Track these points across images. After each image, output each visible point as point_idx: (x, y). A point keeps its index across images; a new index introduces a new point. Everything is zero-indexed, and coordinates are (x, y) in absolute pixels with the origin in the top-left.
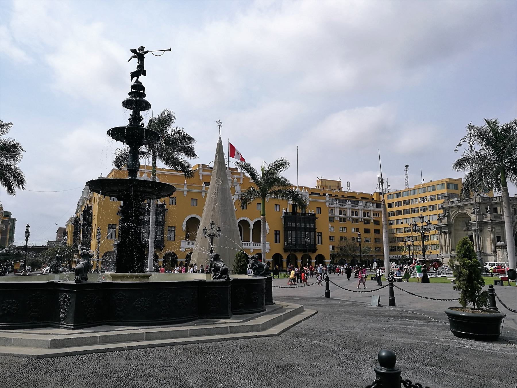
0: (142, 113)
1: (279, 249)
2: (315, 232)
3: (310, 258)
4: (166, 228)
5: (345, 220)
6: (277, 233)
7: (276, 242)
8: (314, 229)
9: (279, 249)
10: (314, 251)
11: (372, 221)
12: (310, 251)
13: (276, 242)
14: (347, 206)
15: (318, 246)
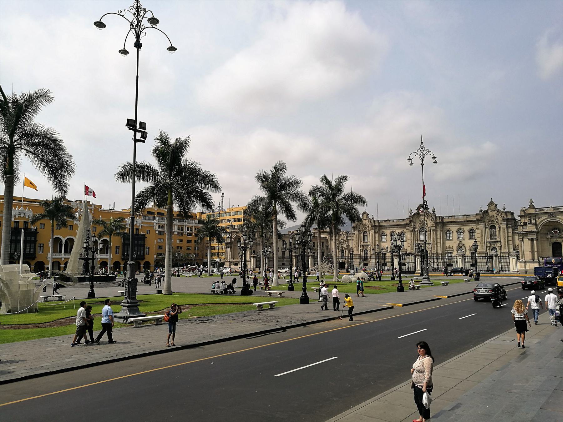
1: (118, 258)
2: (144, 246)
3: (140, 264)
4: (37, 245)
5: (182, 234)
6: (117, 247)
7: (116, 253)
8: (144, 245)
9: (118, 258)
10: (143, 259)
12: (140, 259)
13: (116, 253)
14: (184, 224)
15: (147, 256)
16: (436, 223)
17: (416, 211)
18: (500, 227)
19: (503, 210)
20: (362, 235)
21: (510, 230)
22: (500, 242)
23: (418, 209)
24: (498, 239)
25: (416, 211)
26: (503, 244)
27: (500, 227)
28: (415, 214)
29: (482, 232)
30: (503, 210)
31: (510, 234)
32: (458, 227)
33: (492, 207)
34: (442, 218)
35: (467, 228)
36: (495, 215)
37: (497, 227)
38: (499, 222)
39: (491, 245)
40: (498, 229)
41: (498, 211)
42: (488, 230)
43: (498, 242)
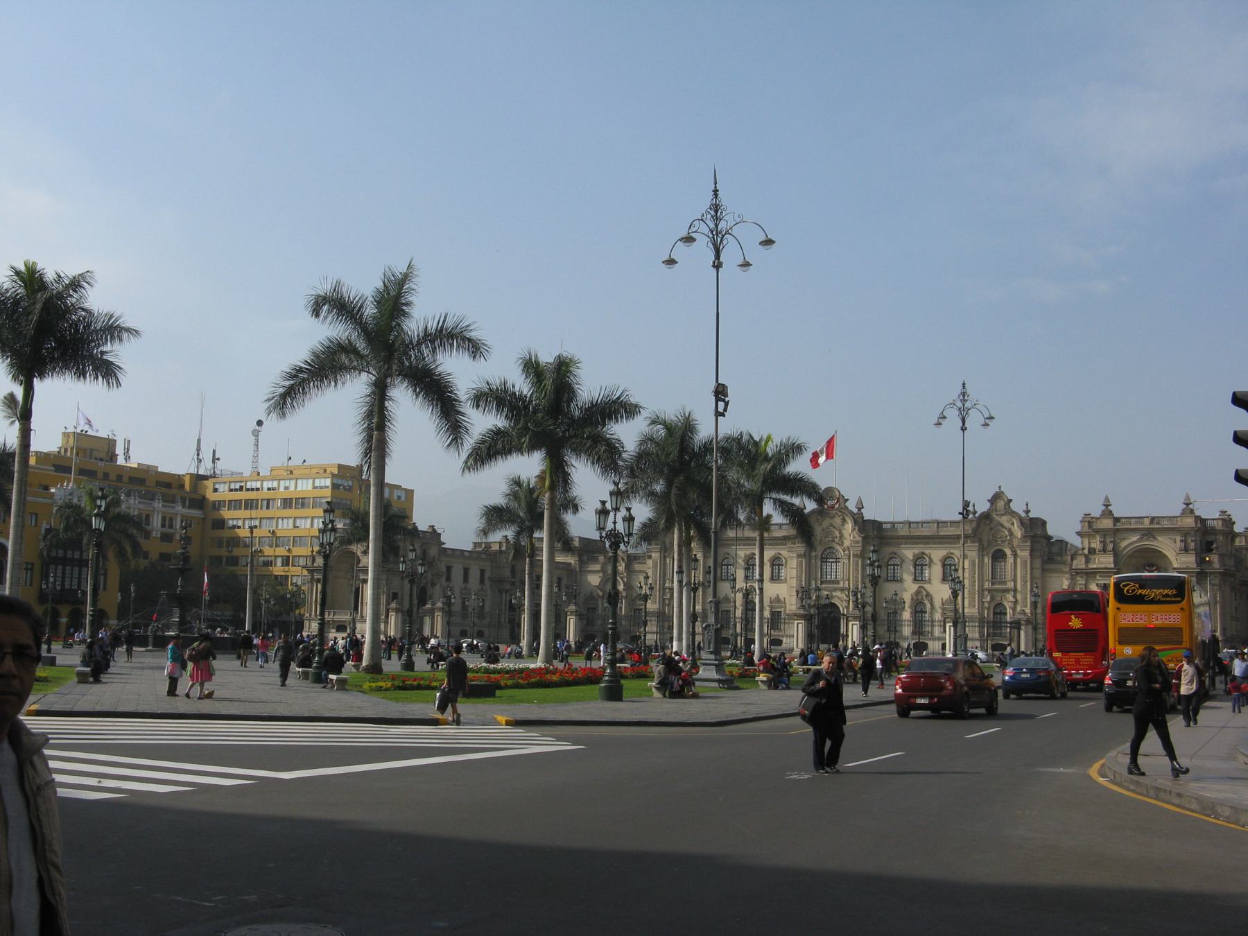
11: (178, 537)
16: (866, 540)
18: (1015, 556)
19: (1023, 515)
21: (1038, 562)
22: (1015, 590)
24: (1010, 585)
26: (1019, 596)
27: (1015, 556)
30: (1023, 515)
31: (1038, 573)
32: (917, 551)
33: (1000, 504)
35: (937, 554)
36: (1007, 525)
37: (1008, 552)
38: (1015, 542)
39: (992, 598)
40: (1010, 560)
41: (1013, 514)
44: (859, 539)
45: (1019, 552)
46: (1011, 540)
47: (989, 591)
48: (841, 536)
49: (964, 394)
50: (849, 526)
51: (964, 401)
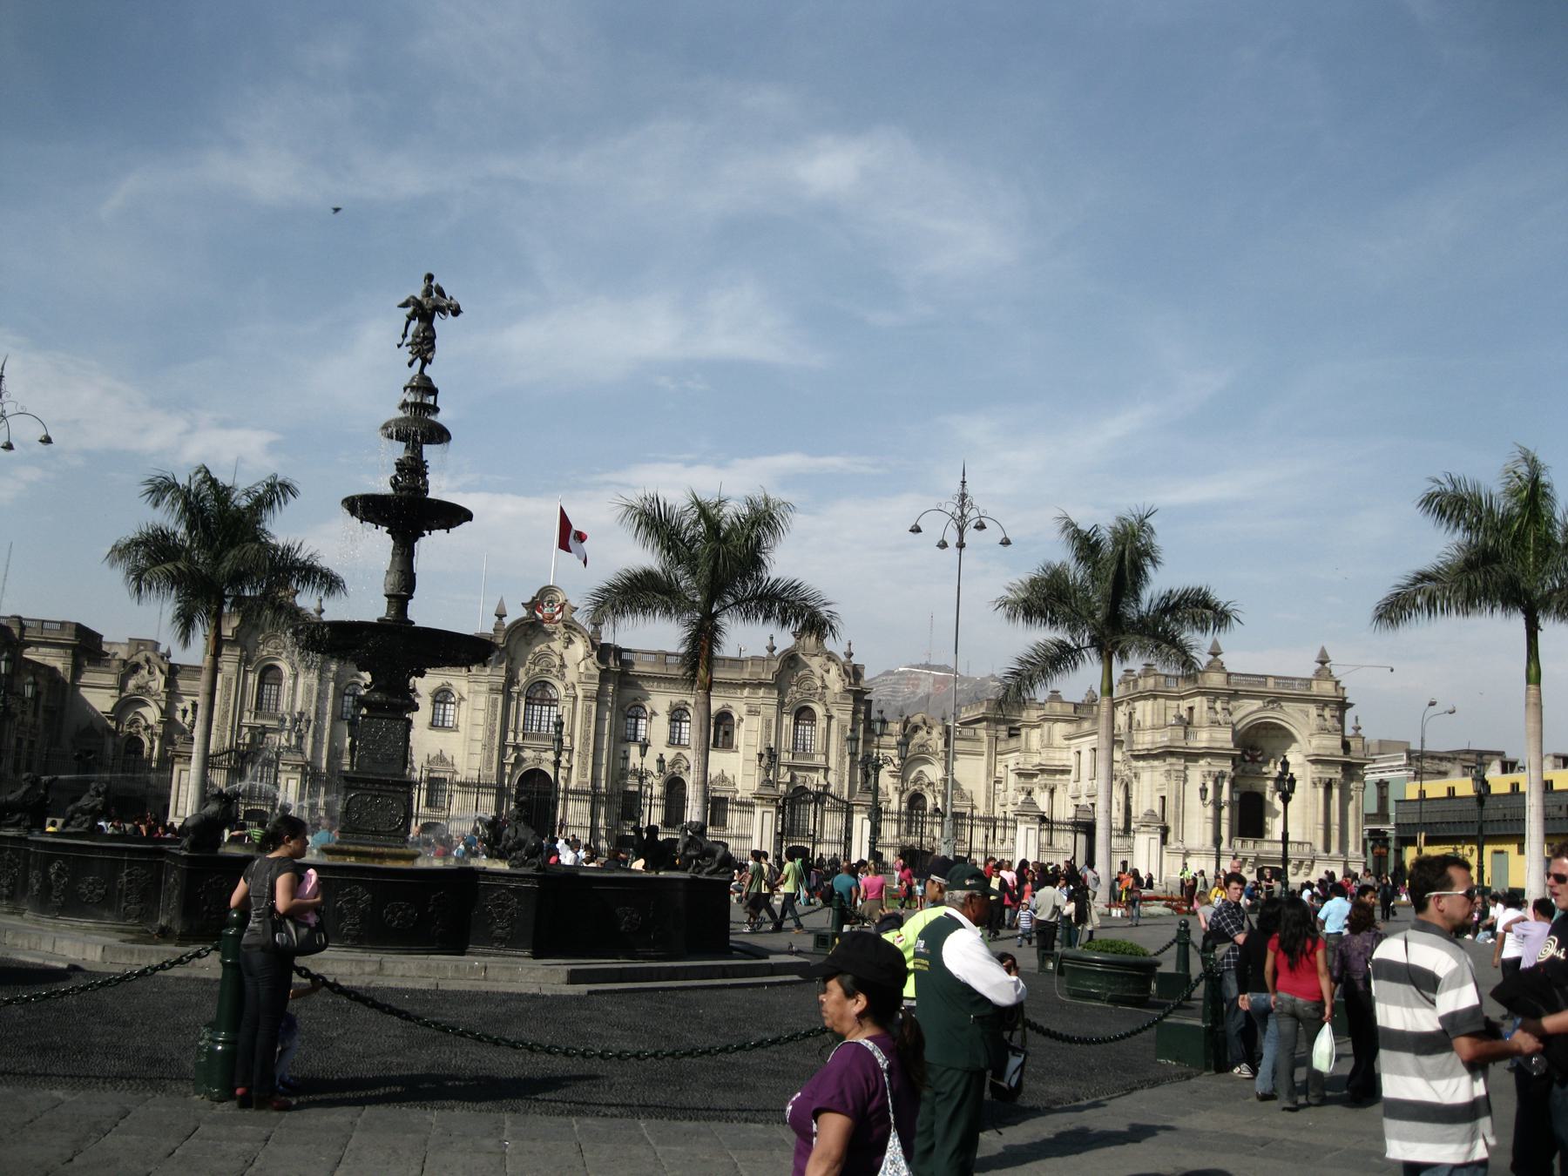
0: (430, 452)
16: (605, 676)
17: (523, 613)
20: (252, 679)
23: (533, 605)
24: (819, 760)
25: (523, 613)
27: (830, 718)
28: (518, 625)
29: (768, 726)
32: (676, 699)
34: (619, 652)
37: (819, 710)
38: (829, 699)
40: (821, 723)
42: (788, 721)
43: (815, 769)
44: (597, 673)
45: (834, 712)
46: (823, 694)
47: (789, 767)
48: (563, 666)
49: (963, 496)
50: (579, 648)
51: (962, 506)
